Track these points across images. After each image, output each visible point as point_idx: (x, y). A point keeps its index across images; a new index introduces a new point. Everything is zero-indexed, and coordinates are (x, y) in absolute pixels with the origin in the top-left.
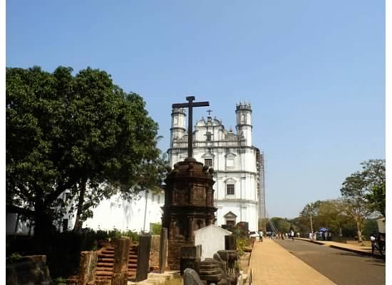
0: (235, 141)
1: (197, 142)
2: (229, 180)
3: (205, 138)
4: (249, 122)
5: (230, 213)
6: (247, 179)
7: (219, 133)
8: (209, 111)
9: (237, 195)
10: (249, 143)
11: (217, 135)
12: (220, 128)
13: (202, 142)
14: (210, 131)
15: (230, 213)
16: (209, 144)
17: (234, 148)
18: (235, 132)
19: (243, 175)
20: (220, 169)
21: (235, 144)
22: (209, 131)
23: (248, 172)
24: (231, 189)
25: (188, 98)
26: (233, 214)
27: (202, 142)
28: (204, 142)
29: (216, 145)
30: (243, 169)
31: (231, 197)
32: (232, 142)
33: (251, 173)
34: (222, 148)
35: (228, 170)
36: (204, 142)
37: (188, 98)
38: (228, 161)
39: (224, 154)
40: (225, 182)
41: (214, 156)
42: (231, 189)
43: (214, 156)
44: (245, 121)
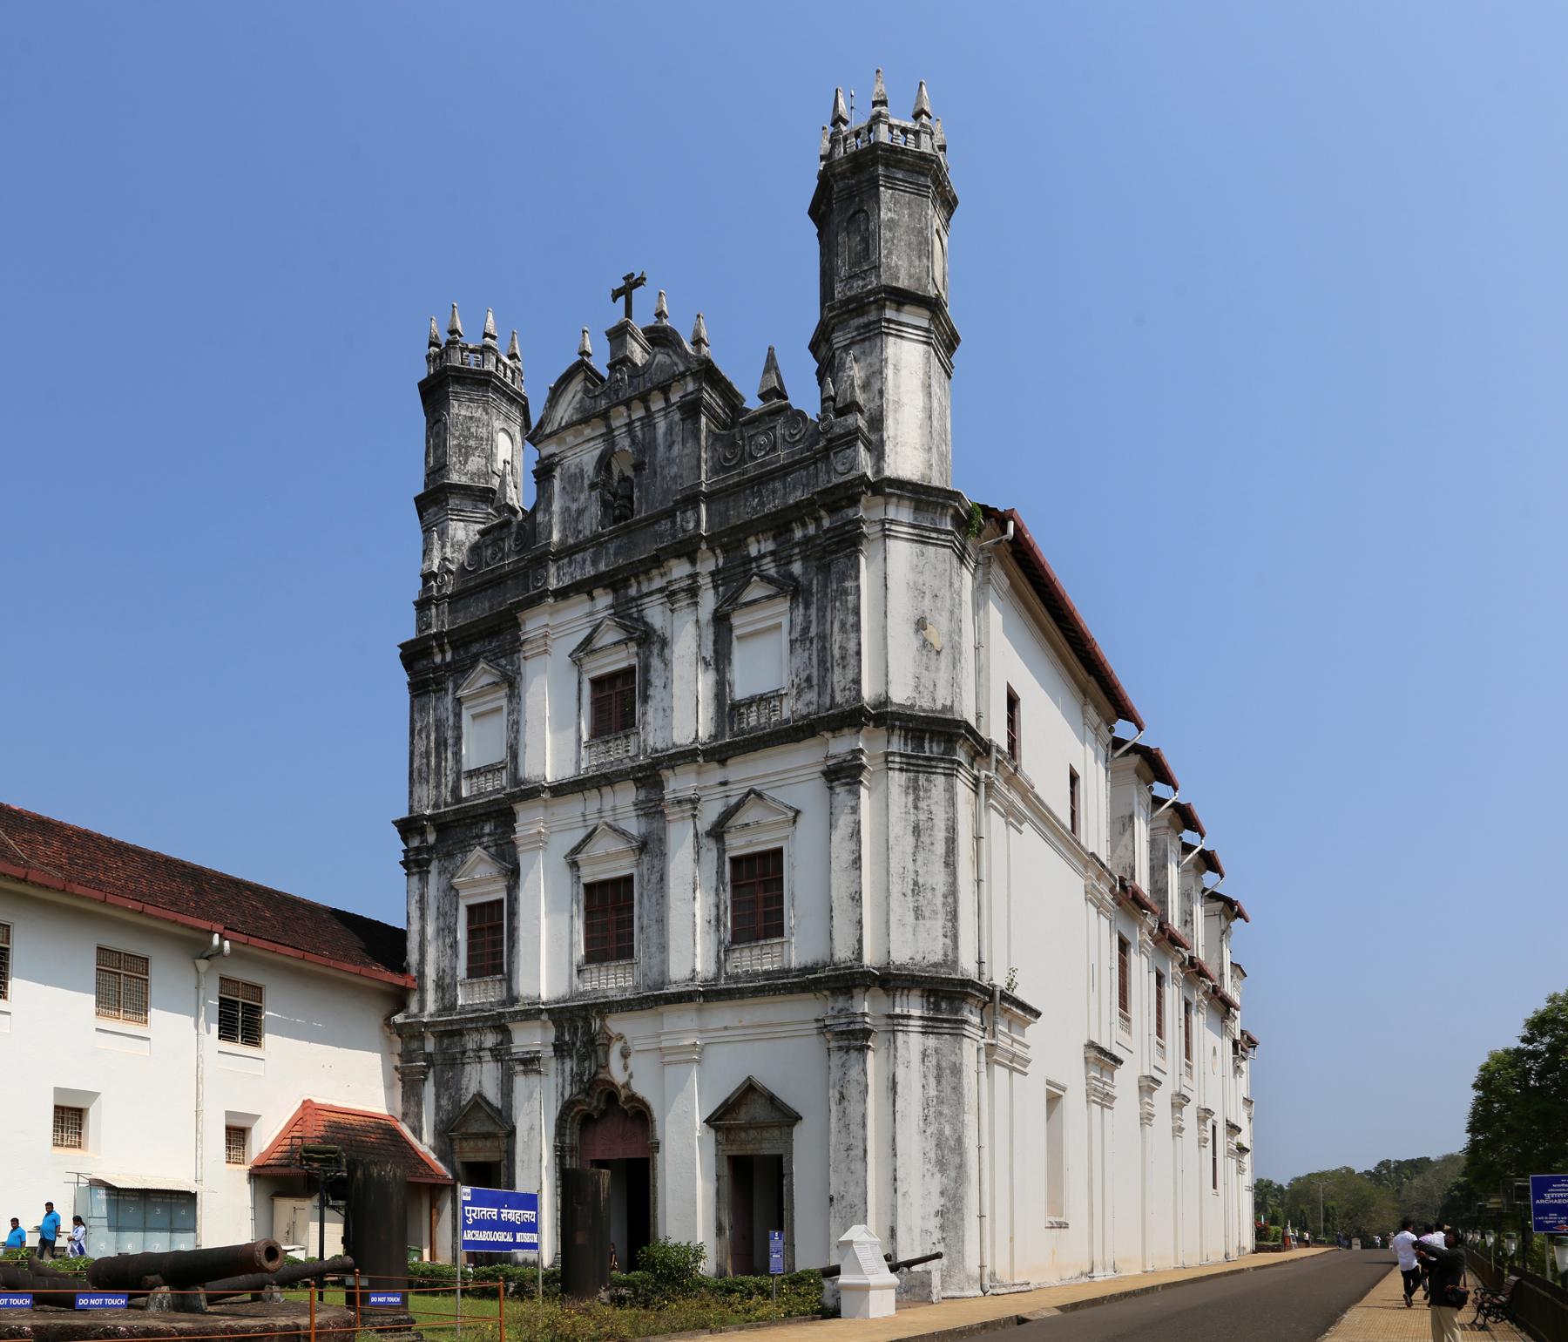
2: (750, 815)
5: (750, 1089)
15: (750, 1089)
18: (805, 397)
24: (755, 892)
26: (772, 1100)
31: (757, 960)
38: (739, 653)
39: (708, 601)
40: (718, 832)
42: (755, 892)
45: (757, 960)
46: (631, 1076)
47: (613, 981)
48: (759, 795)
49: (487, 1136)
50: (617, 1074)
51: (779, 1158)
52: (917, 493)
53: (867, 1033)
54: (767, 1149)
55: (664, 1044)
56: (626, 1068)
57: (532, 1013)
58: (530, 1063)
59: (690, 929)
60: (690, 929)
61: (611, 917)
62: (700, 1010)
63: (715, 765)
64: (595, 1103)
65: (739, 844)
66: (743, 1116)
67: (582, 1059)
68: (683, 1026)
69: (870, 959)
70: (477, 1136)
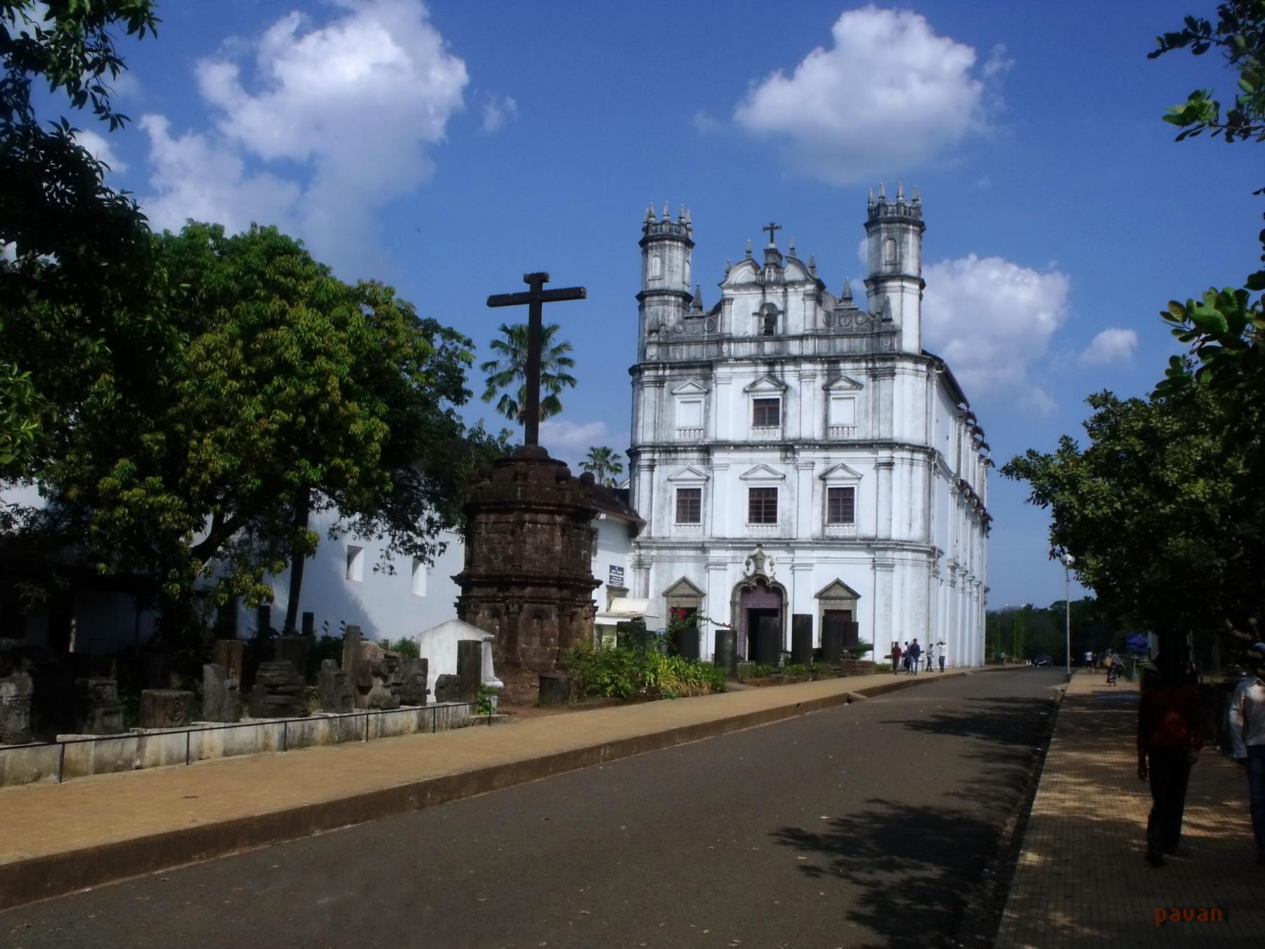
0: (862, 336)
1: (730, 340)
2: (840, 473)
3: (752, 327)
4: (910, 267)
6: (897, 468)
7: (804, 300)
8: (772, 228)
9: (865, 522)
10: (910, 343)
11: (799, 313)
12: (810, 287)
13: (742, 340)
14: (774, 297)
15: (838, 583)
16: (769, 347)
17: (855, 358)
19: (884, 455)
20: (806, 434)
21: (861, 345)
22: (769, 299)
23: (902, 446)
24: (841, 504)
25: (529, 279)
26: (847, 589)
27: (742, 340)
28: (751, 340)
29: (794, 348)
30: (885, 435)
32: (849, 336)
33: (914, 449)
34: (811, 359)
35: (833, 436)
36: (751, 340)
37: (529, 279)
38: (834, 404)
39: (820, 381)
40: (823, 478)
41: (785, 391)
42: (841, 504)
43: (786, 389)
44: (897, 263)
48: (844, 467)
50: (768, 572)
51: (849, 612)
53: (893, 566)
54: (844, 605)
57: (722, 543)
58: (721, 565)
61: (763, 505)
65: (832, 484)
67: (748, 564)
68: (801, 555)
69: (895, 536)
70: (683, 596)
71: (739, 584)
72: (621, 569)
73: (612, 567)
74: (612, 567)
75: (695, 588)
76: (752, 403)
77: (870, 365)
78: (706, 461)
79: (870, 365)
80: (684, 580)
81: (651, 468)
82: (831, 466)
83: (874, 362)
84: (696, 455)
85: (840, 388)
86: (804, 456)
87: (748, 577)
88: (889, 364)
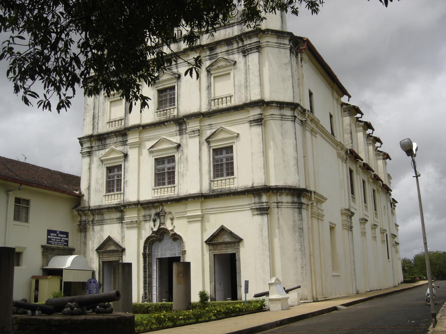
5: (222, 230)
15: (222, 230)
19: (255, 113)
20: (194, 109)
24: (223, 162)
26: (231, 233)
33: (281, 105)
40: (208, 140)
42: (223, 162)
45: (224, 184)
46: (174, 227)
47: (166, 193)
49: (113, 251)
50: (168, 226)
52: (277, 33)
55: (188, 215)
56: (172, 224)
59: (193, 175)
60: (193, 175)
62: (202, 202)
63: (207, 118)
64: (159, 237)
66: (221, 240)
67: (154, 221)
71: (148, 239)
72: (67, 234)
73: (50, 232)
74: (50, 232)
75: (117, 244)
76: (156, 92)
77: (240, 45)
78: (124, 143)
79: (240, 45)
80: (109, 240)
81: (89, 154)
82: (213, 131)
83: (243, 41)
84: (115, 139)
85: (219, 68)
86: (193, 125)
87: (153, 232)
88: (255, 40)
